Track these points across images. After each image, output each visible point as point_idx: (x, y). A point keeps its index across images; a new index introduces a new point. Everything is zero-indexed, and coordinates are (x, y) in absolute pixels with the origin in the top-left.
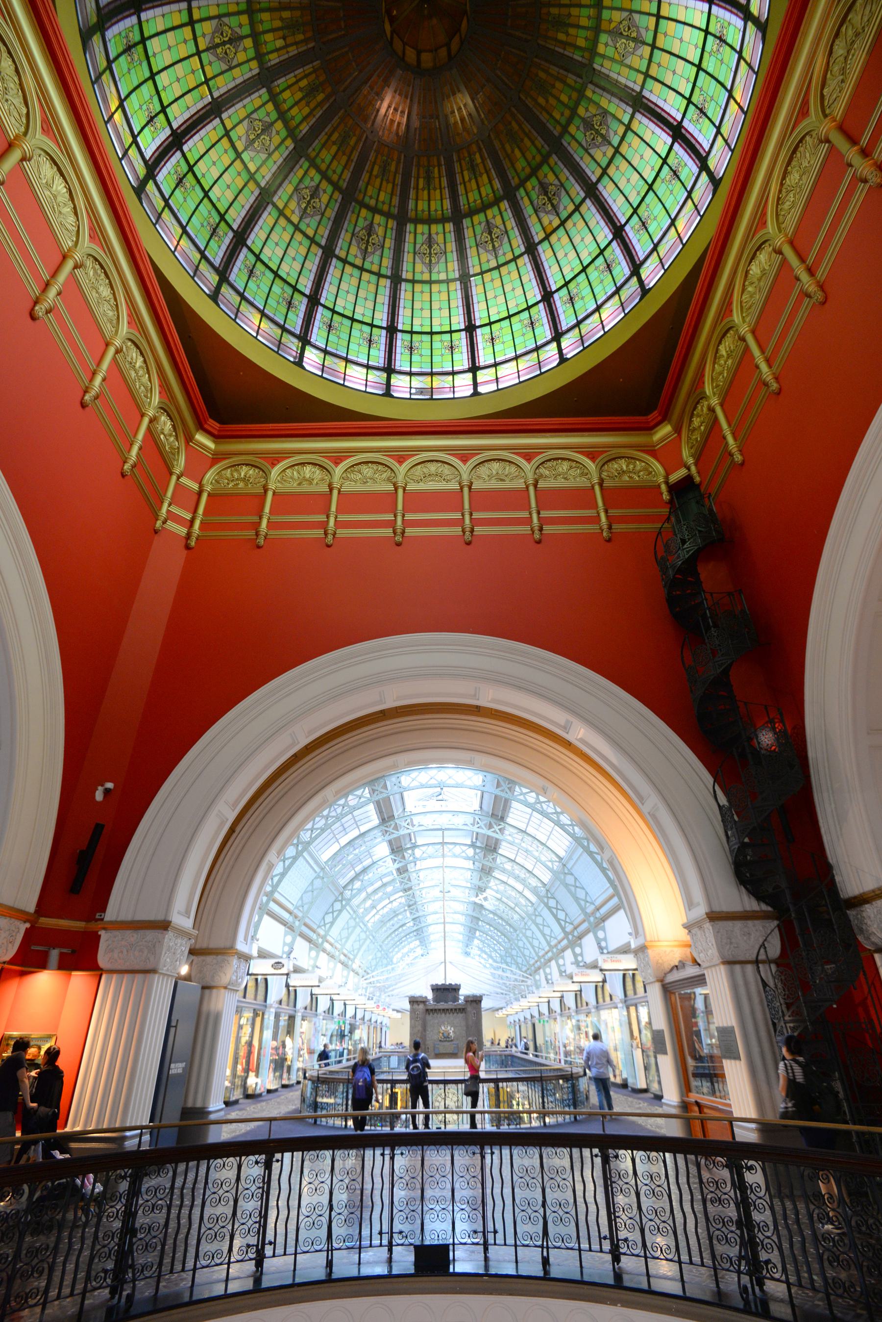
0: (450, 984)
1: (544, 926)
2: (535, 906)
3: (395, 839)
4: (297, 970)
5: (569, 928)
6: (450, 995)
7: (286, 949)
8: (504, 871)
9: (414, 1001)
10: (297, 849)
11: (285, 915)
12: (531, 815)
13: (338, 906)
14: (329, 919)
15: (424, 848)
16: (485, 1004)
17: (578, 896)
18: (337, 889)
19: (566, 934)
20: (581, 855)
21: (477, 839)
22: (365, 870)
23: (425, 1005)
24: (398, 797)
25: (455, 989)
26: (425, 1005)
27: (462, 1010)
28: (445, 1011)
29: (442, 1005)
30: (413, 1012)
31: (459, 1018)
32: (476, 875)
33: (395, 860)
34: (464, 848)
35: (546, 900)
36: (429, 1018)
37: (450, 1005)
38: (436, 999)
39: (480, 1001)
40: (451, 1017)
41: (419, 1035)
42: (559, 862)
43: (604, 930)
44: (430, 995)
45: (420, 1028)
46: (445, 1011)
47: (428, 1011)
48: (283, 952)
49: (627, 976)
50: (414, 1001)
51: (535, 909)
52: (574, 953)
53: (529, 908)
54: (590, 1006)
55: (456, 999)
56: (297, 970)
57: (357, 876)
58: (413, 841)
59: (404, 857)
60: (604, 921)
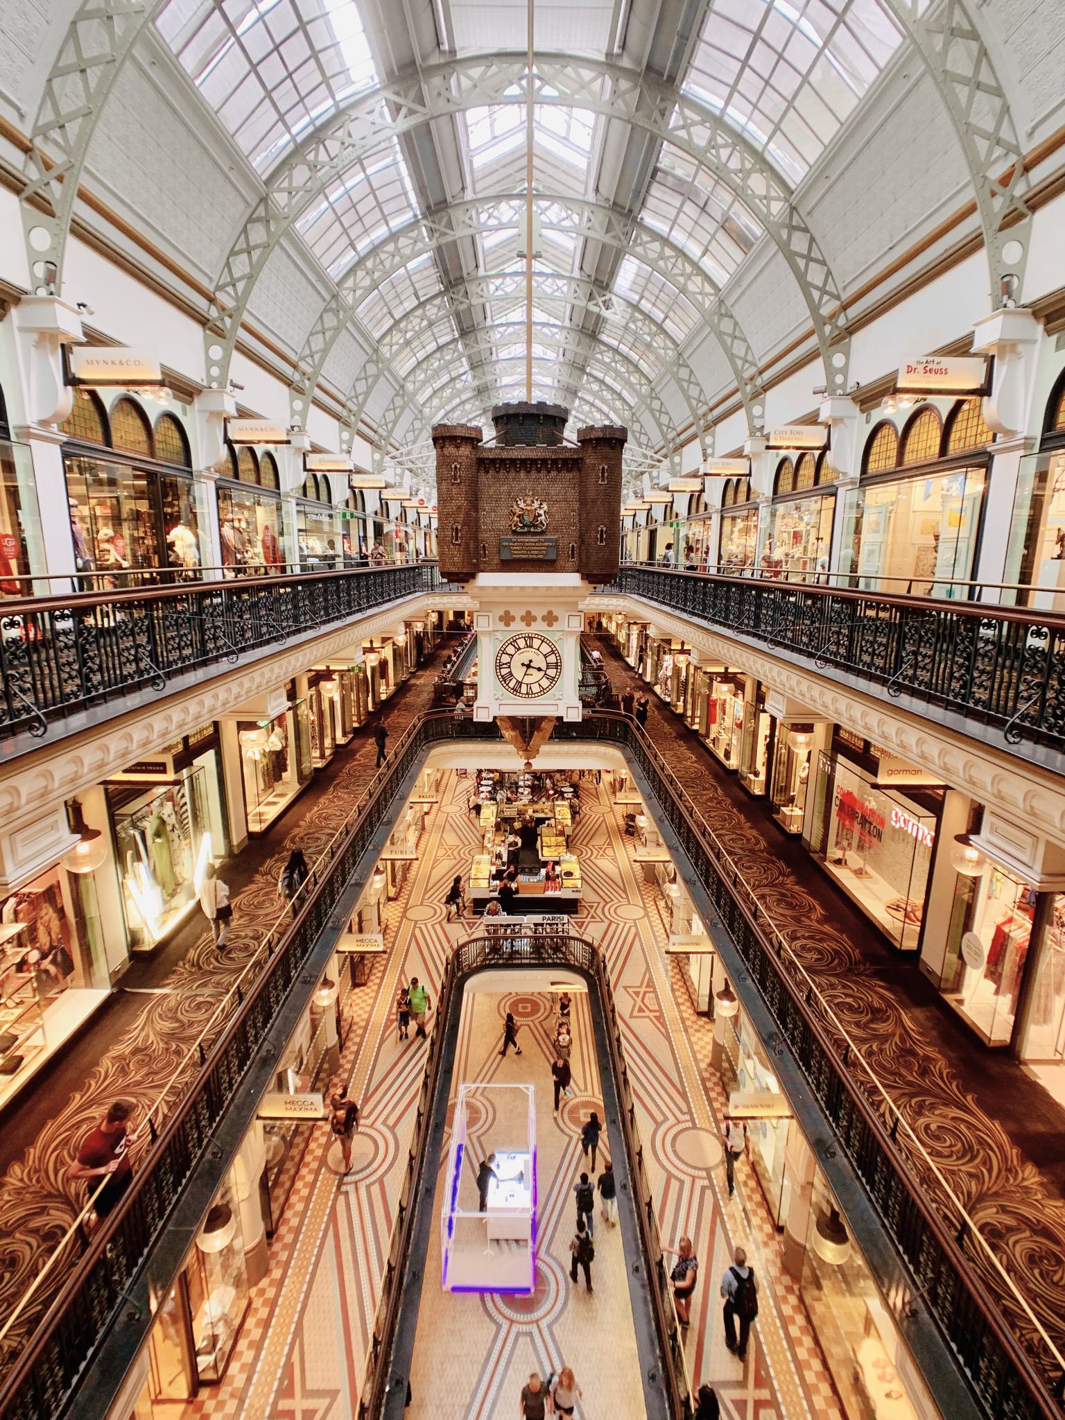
0: (541, 405)
1: (809, 258)
2: (794, 199)
3: (447, 244)
4: (316, 450)
5: (828, 307)
6: (541, 432)
7: (40, 270)
8: (687, 148)
9: (444, 438)
10: (268, 230)
11: (201, 303)
12: (680, 210)
13: (371, 369)
14: (241, 266)
15: (476, 72)
16: (631, 454)
17: (734, 351)
18: (371, 345)
19: (820, 321)
20: (775, 254)
21: (623, 46)
22: (318, 135)
23: (475, 448)
24: (468, 242)
25: (552, 419)
26: (475, 448)
27: (571, 463)
28: (527, 465)
29: (519, 452)
30: (443, 463)
31: (562, 486)
32: (600, 218)
33: (398, 108)
34: (587, 74)
35: (784, 234)
36: (485, 479)
37: (539, 451)
38: (505, 439)
39: (621, 442)
40: (543, 481)
41: (461, 518)
42: (786, 200)
43: (763, 405)
44: (489, 435)
45: (462, 502)
46: (527, 465)
47: (485, 464)
48: (210, 378)
49: (807, 458)
50: (444, 438)
51: (652, 389)
52: (828, 366)
53: (670, 353)
54: (710, 510)
55: (555, 439)
56: (316, 450)
57: (299, 150)
58: (446, 47)
59: (421, 100)
60: (765, 391)
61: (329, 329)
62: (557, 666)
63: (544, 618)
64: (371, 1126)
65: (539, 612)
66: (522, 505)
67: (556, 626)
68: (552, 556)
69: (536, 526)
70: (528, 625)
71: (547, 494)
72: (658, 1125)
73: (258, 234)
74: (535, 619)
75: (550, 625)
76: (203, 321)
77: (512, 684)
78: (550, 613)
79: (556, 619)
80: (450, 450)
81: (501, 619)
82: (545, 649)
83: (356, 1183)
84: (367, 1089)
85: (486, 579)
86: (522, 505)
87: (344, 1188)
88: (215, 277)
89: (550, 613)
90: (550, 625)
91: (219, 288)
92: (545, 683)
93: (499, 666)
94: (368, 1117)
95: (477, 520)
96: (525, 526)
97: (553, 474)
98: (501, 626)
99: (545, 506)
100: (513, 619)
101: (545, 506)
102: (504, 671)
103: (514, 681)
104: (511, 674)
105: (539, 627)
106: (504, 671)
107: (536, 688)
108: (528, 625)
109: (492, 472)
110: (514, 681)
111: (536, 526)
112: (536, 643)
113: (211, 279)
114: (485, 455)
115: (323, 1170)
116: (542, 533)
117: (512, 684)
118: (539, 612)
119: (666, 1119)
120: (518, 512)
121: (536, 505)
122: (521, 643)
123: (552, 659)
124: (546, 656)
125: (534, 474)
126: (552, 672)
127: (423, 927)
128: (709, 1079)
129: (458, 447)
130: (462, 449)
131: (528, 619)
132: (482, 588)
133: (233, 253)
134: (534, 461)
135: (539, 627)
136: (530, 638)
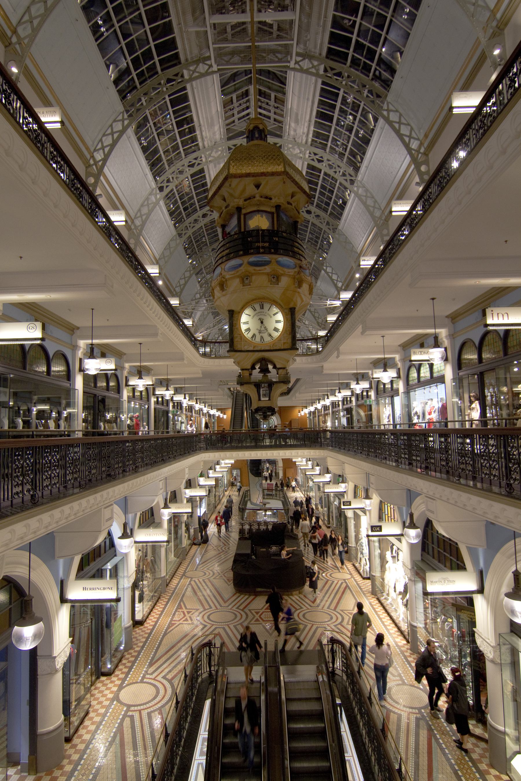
64: (154, 679)
83: (140, 711)
84: (153, 658)
94: (152, 674)
115: (115, 702)
127: (197, 580)
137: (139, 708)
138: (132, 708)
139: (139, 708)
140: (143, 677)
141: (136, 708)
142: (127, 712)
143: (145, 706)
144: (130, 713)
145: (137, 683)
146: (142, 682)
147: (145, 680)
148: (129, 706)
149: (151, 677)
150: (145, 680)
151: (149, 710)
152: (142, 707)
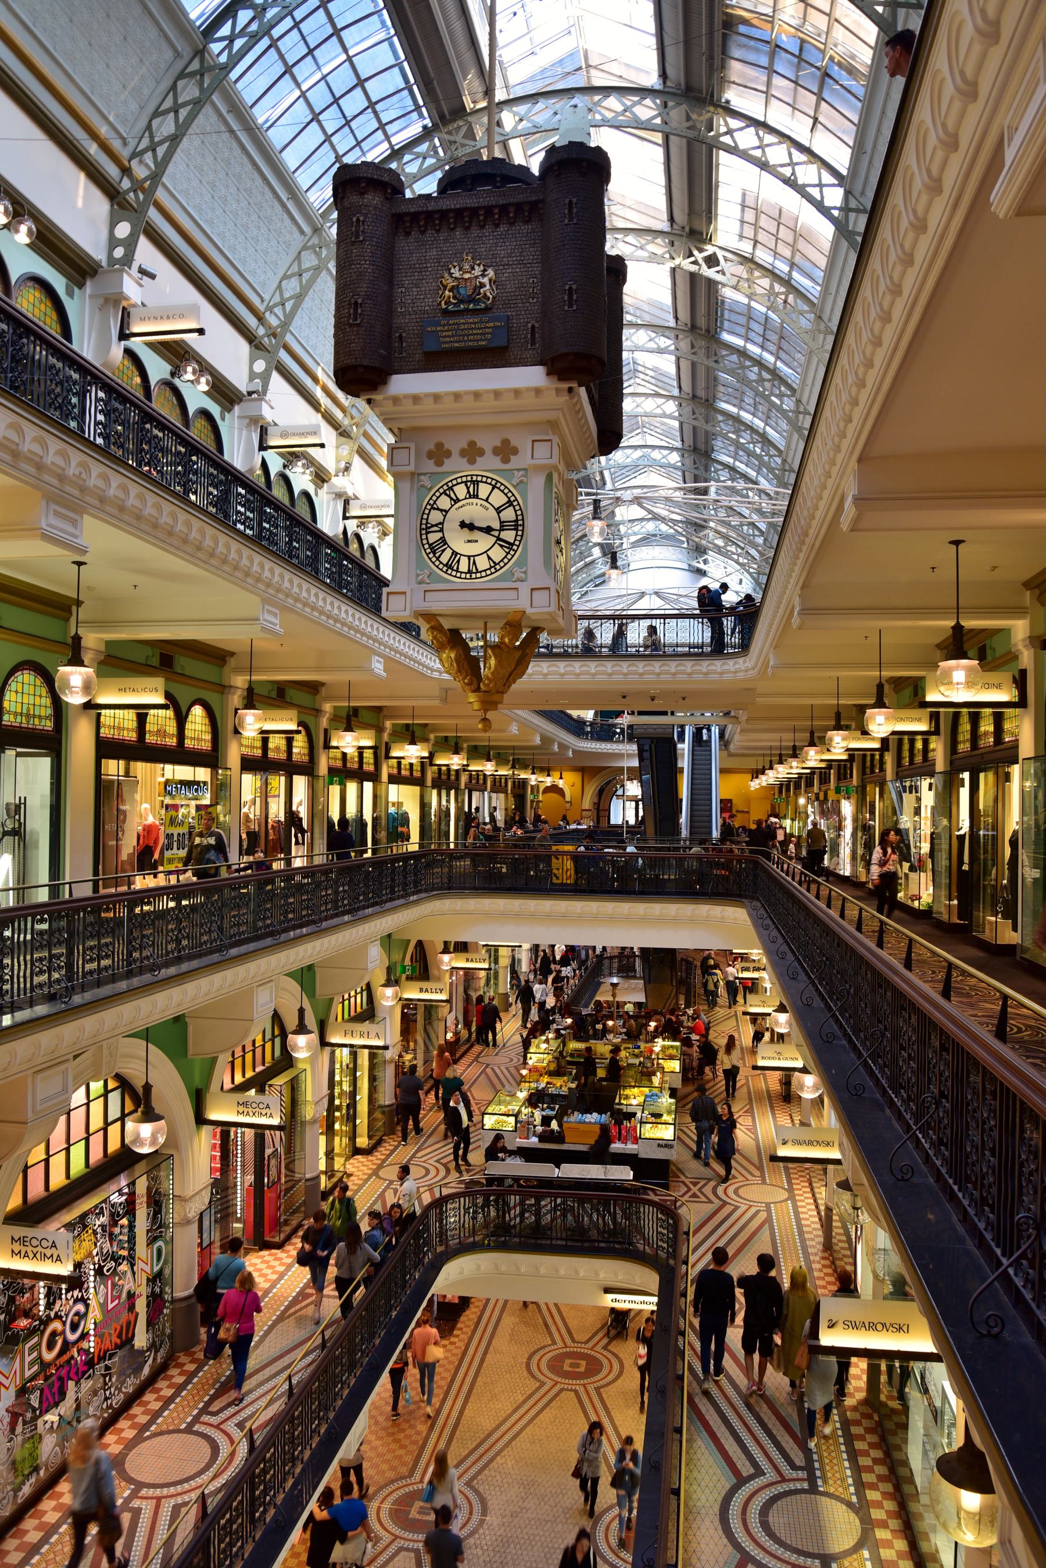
61: (307, 270)
62: (517, 525)
63: (496, 451)
65: (488, 442)
66: (457, 273)
67: (515, 462)
68: (501, 342)
69: (476, 302)
70: (472, 462)
71: (494, 256)
72: (741, 1481)
73: (189, 91)
74: (481, 453)
75: (506, 460)
76: (111, 192)
77: (445, 558)
78: (506, 442)
79: (515, 451)
80: (354, 199)
81: (430, 455)
82: (498, 499)
83: (159, 1499)
85: (402, 384)
86: (457, 273)
87: (136, 1503)
88: (132, 143)
89: (506, 442)
90: (506, 460)
91: (134, 155)
92: (497, 553)
93: (426, 528)
95: (390, 299)
96: (461, 301)
97: (503, 228)
98: (430, 466)
99: (491, 273)
100: (448, 454)
101: (491, 273)
102: (433, 537)
103: (448, 553)
104: (443, 541)
105: (487, 465)
106: (433, 537)
107: (482, 563)
108: (472, 462)
109: (414, 234)
110: (448, 553)
111: (476, 302)
112: (484, 490)
113: (125, 143)
114: (404, 209)
116: (487, 310)
117: (445, 558)
118: (488, 442)
119: (759, 1472)
120: (450, 283)
121: (478, 270)
122: (461, 491)
123: (509, 514)
124: (499, 510)
125: (475, 232)
126: (509, 535)
128: (858, 1423)
129: (362, 194)
130: (369, 197)
131: (472, 453)
132: (396, 400)
133: (156, 114)
134: (474, 211)
135: (487, 465)
136: (476, 483)
137: (158, 1492)
138: (144, 1492)
139: (158, 1492)
140: (196, 1420)
141: (151, 1492)
142: (134, 1495)
143: (172, 1490)
144: (136, 1503)
145: (179, 1431)
146: (189, 1430)
147: (196, 1428)
148: (140, 1485)
149: (214, 1420)
150: (196, 1428)
151: (179, 1500)
152: (165, 1491)
